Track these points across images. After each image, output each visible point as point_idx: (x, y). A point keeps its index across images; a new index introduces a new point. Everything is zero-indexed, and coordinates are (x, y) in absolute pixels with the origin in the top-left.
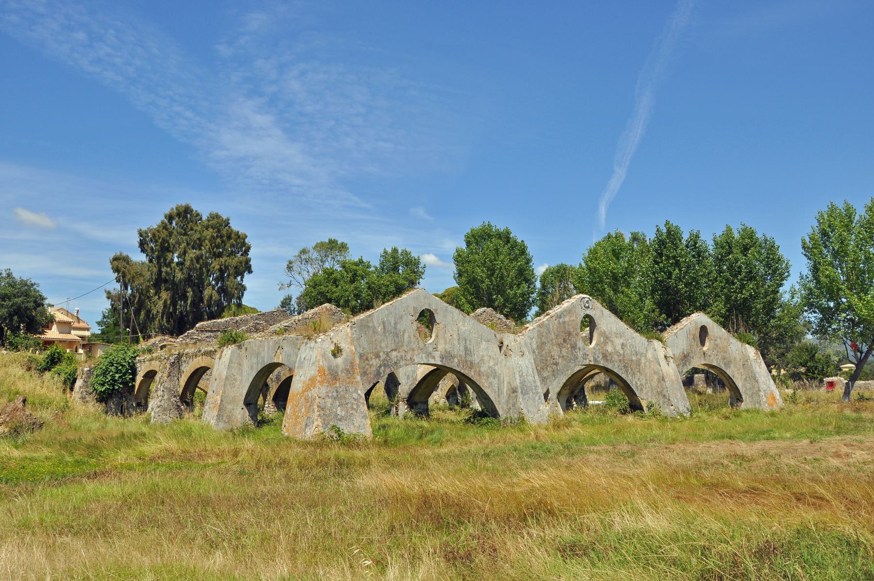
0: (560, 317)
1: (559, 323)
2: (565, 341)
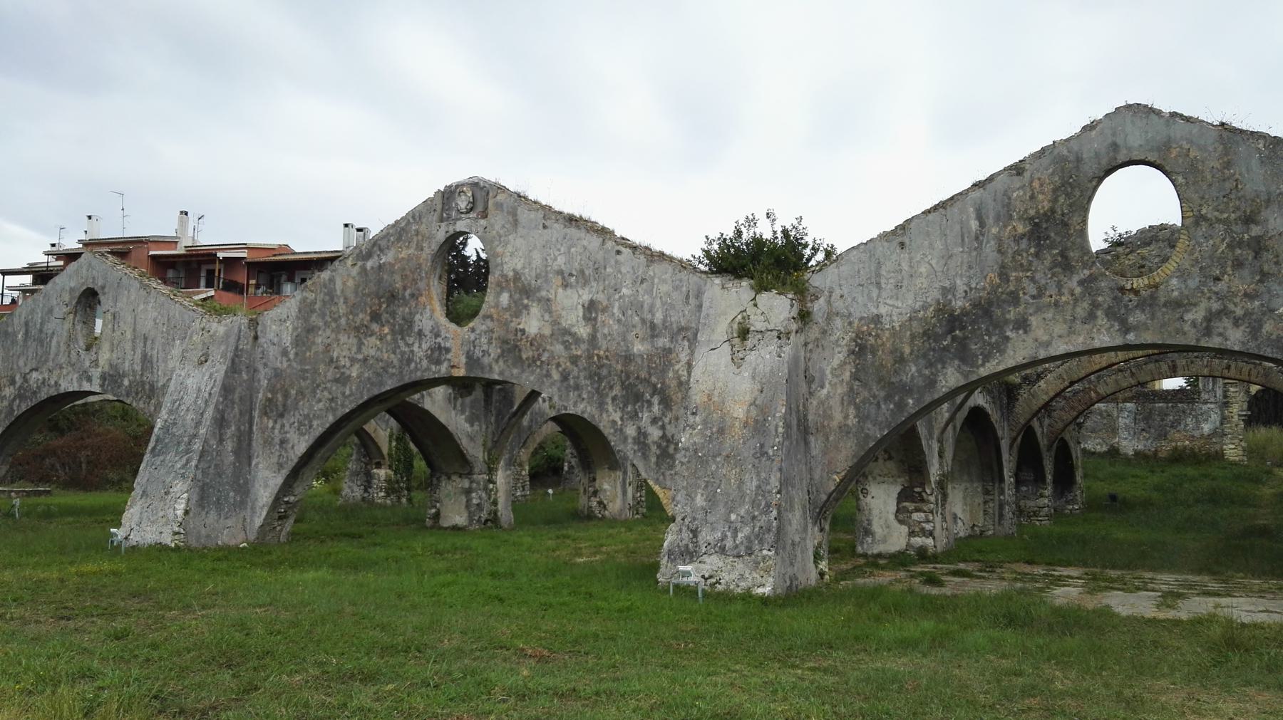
0: (369, 255)
1: (363, 269)
2: (375, 317)
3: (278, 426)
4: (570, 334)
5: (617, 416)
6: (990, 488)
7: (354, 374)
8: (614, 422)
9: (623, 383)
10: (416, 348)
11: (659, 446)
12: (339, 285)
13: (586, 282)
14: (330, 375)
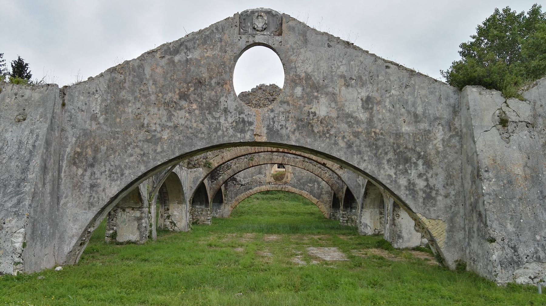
1: (171, 62)
3: (88, 173)
4: (352, 117)
5: (392, 172)
6: (382, 211)
7: (166, 137)
8: (390, 176)
9: (395, 151)
10: (222, 120)
11: (425, 192)
12: (148, 71)
13: (363, 85)
14: (141, 136)
